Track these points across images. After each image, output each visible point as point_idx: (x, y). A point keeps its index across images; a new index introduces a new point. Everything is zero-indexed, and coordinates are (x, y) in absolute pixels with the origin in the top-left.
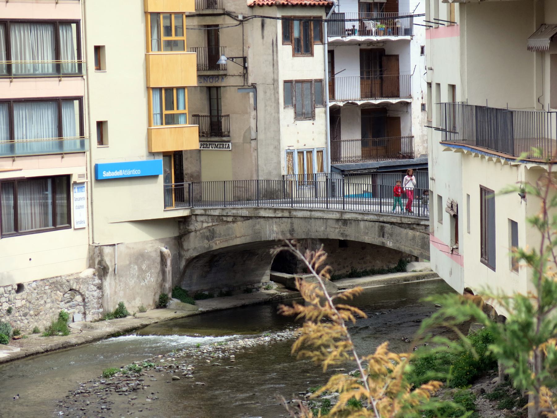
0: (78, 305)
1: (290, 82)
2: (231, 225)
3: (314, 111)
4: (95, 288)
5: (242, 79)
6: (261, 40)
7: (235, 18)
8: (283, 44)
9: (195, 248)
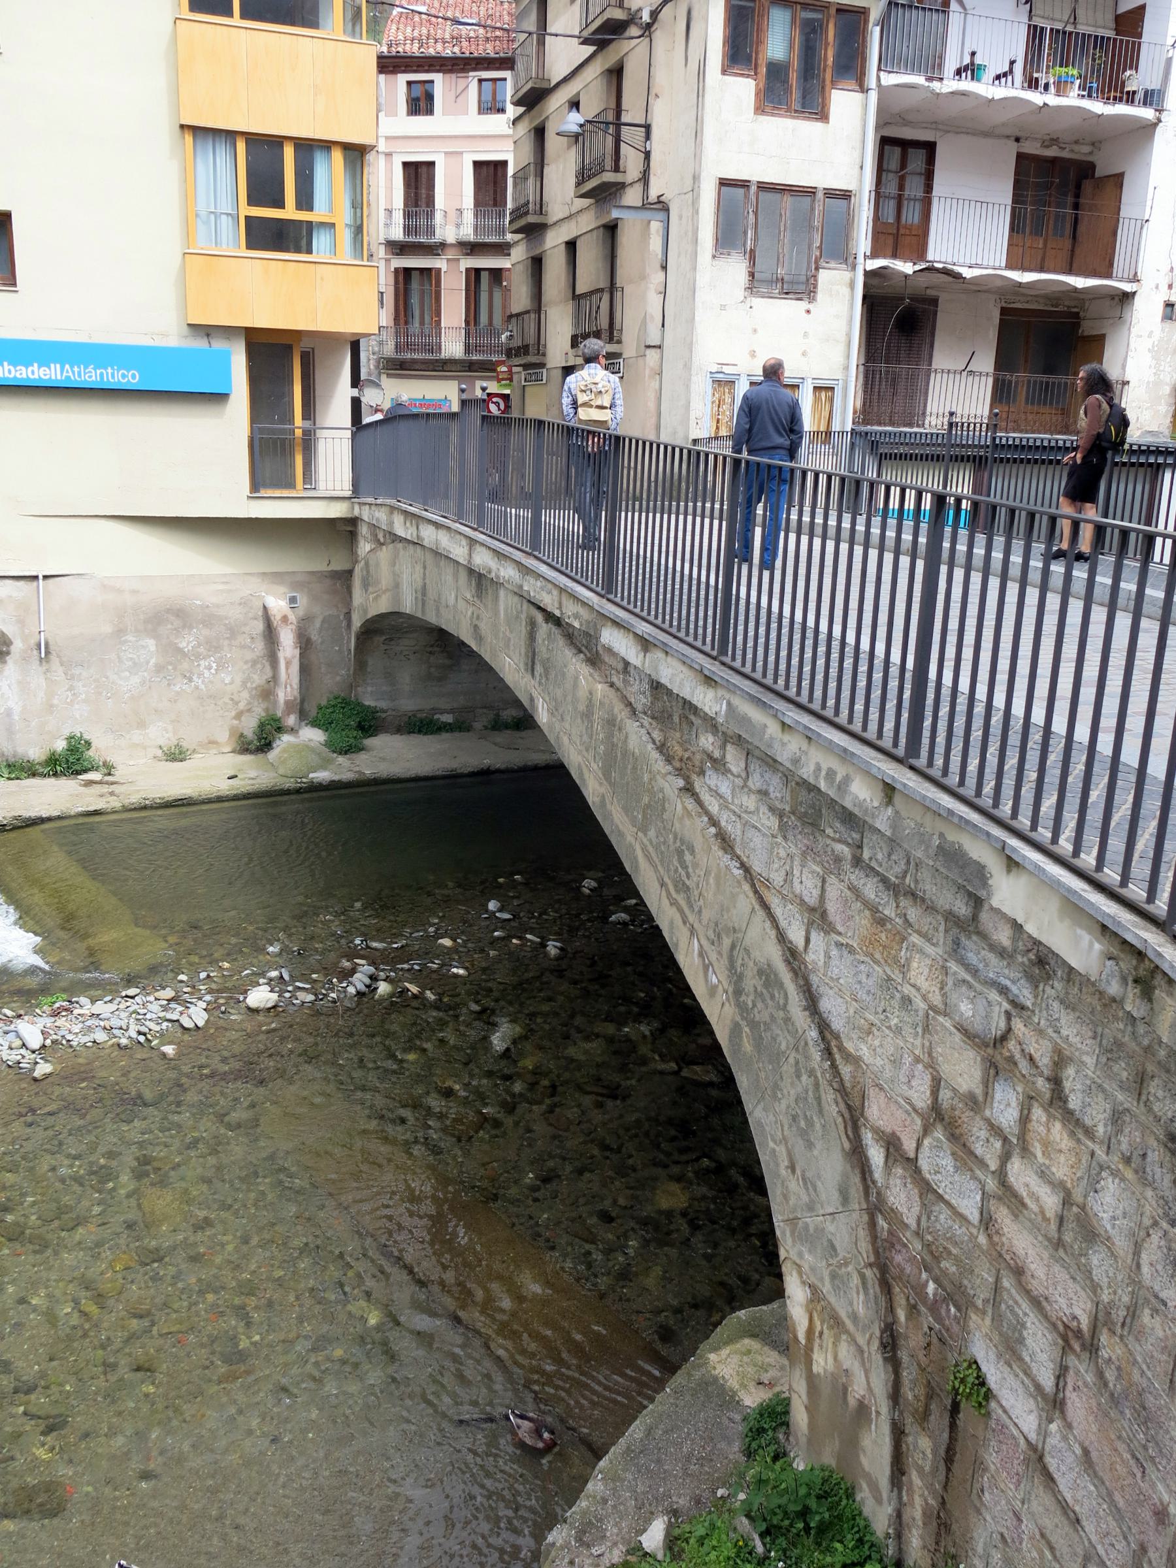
1: (744, 184)
8: (724, 72)
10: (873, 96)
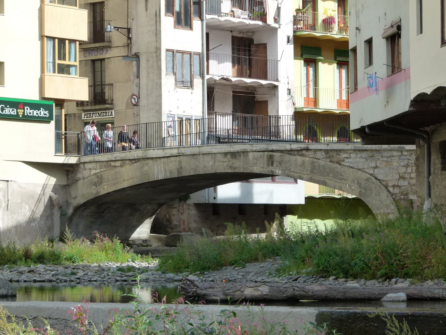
2: (118, 169)
5: (126, 49)
6: (145, 12)
9: (83, 195)
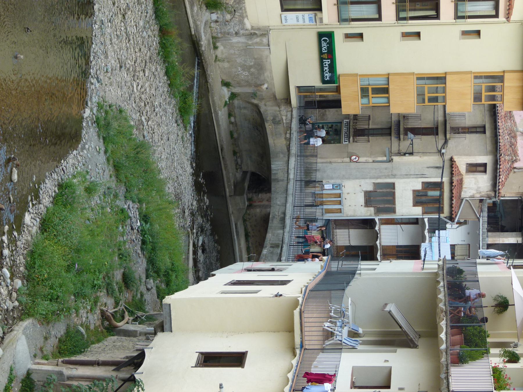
0: (223, 17)
2: (283, 135)
3: (371, 207)
4: (236, 30)
5: (396, 152)
7: (443, 147)
8: (423, 183)
10: (421, 217)
